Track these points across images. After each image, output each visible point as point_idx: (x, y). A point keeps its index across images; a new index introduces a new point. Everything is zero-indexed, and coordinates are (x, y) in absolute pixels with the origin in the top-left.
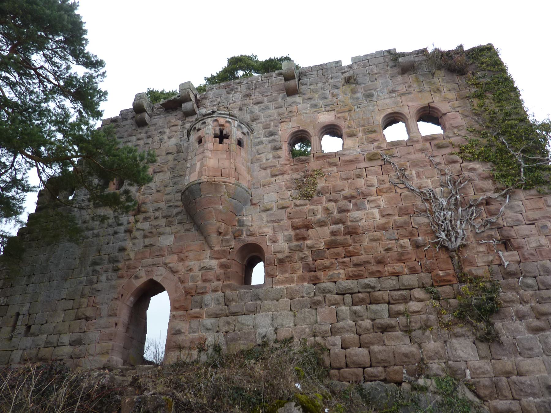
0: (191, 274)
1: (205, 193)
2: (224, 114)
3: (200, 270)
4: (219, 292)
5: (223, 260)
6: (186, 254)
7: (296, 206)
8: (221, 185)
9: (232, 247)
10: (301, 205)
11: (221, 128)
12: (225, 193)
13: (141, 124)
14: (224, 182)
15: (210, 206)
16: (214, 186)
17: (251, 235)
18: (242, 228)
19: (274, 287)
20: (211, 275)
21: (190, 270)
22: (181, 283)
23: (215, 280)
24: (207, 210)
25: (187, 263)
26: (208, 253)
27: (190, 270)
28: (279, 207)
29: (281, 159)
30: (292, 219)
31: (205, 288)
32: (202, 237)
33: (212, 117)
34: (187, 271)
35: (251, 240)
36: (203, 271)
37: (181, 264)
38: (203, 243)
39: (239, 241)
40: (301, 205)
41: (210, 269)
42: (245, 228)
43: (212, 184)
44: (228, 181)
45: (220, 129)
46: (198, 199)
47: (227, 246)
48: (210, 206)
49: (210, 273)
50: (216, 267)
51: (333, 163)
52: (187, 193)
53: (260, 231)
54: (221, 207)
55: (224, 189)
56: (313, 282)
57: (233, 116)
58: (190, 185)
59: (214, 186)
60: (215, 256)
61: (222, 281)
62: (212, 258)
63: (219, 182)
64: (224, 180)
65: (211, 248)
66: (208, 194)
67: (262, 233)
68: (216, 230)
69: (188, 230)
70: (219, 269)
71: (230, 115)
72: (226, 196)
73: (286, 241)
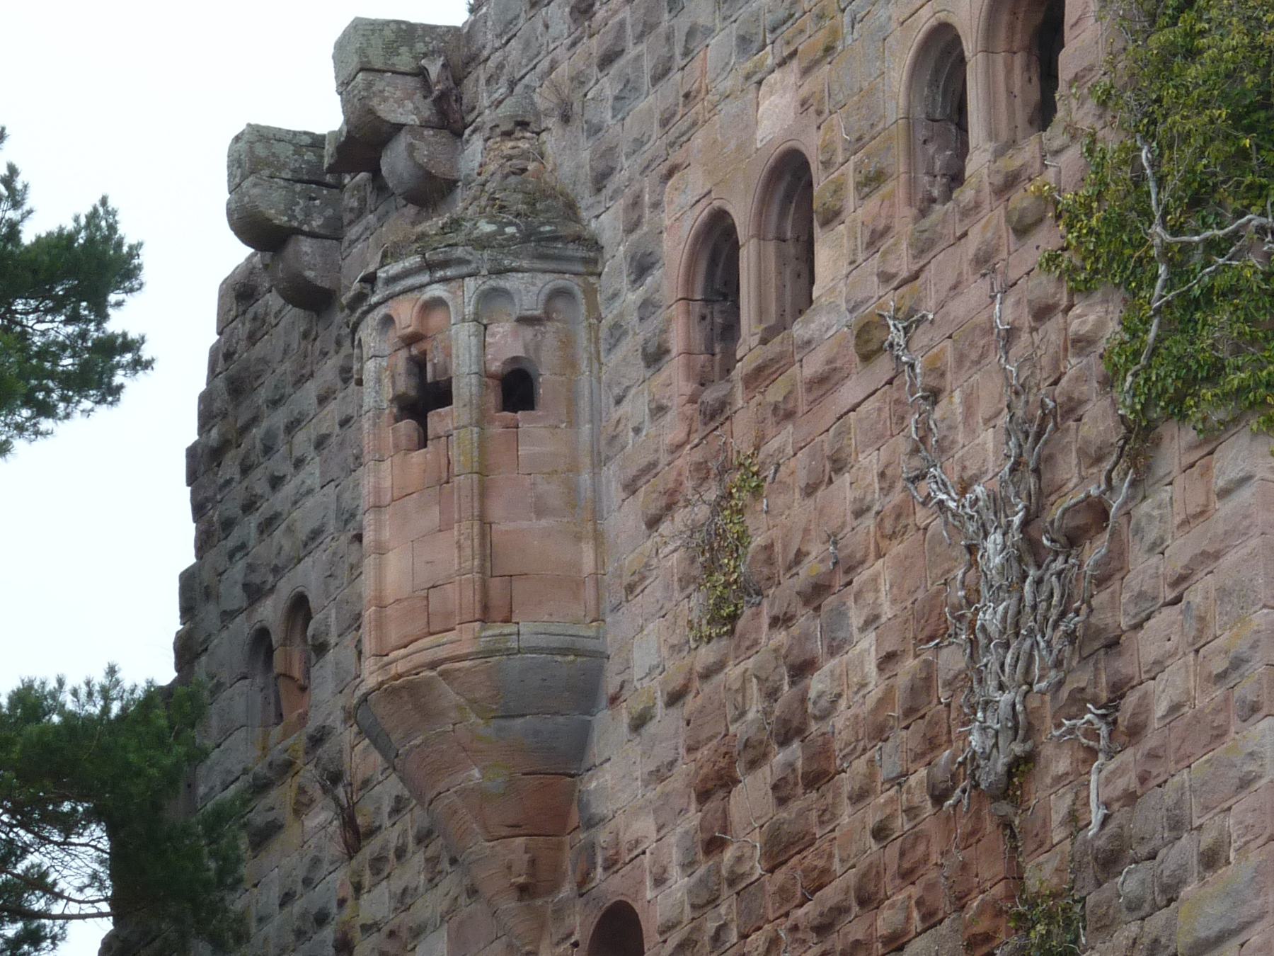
2: (406, 274)
8: (429, 683)
11: (414, 351)
12: (459, 708)
13: (314, 300)
14: (433, 665)
15: (441, 786)
16: (405, 694)
33: (373, 308)
44: (442, 653)
45: (411, 359)
48: (441, 786)
54: (476, 773)
55: (449, 696)
57: (445, 264)
59: (405, 694)
63: (416, 670)
64: (428, 656)
71: (430, 266)
72: (473, 718)
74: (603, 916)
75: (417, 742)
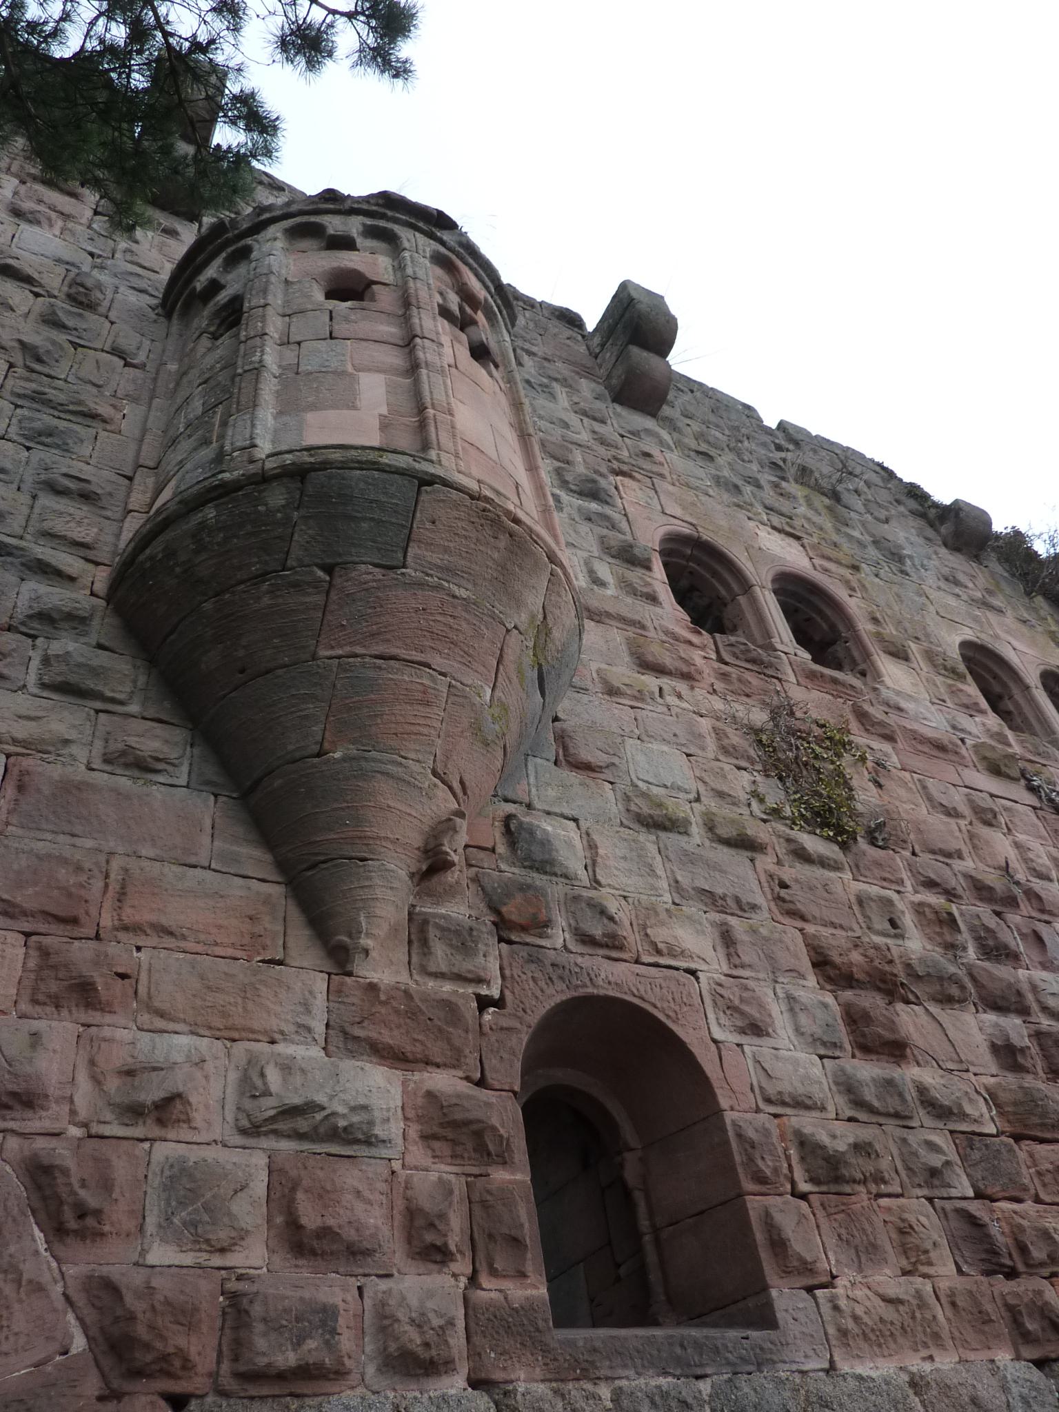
0: (162, 1151)
1: (435, 558)
3: (252, 1130)
4: (455, 1384)
5: (444, 1081)
6: (120, 952)
7: (802, 855)
9: (495, 993)
10: (823, 863)
15: (437, 661)
17: (612, 944)
18: (539, 879)
19: (844, 1367)
20: (362, 1200)
21: (168, 1110)
22: (57, 1232)
23: (394, 1249)
24: (407, 676)
25: (124, 1036)
26: (308, 981)
27: (168, 1110)
28: (724, 832)
29: (658, 610)
30: (803, 918)
31: (326, 1317)
32: (258, 853)
34: (134, 1112)
35: (613, 977)
36: (286, 1145)
37: (60, 1030)
38: (267, 900)
39: (531, 960)
40: (823, 863)
41: (350, 1137)
42: (556, 890)
43: (496, 523)
46: (367, 573)
47: (459, 978)
49: (349, 1177)
50: (394, 1129)
51: (882, 724)
52: (276, 497)
53: (660, 934)
56: (1036, 1354)
58: (337, 456)
60: (387, 1037)
61: (462, 1266)
62: (346, 1039)
65: (340, 958)
66: (449, 571)
67: (672, 954)
68: (416, 840)
69: (142, 766)
70: (418, 1155)
73: (816, 1040)
74: (573, 999)
75: (455, 589)
